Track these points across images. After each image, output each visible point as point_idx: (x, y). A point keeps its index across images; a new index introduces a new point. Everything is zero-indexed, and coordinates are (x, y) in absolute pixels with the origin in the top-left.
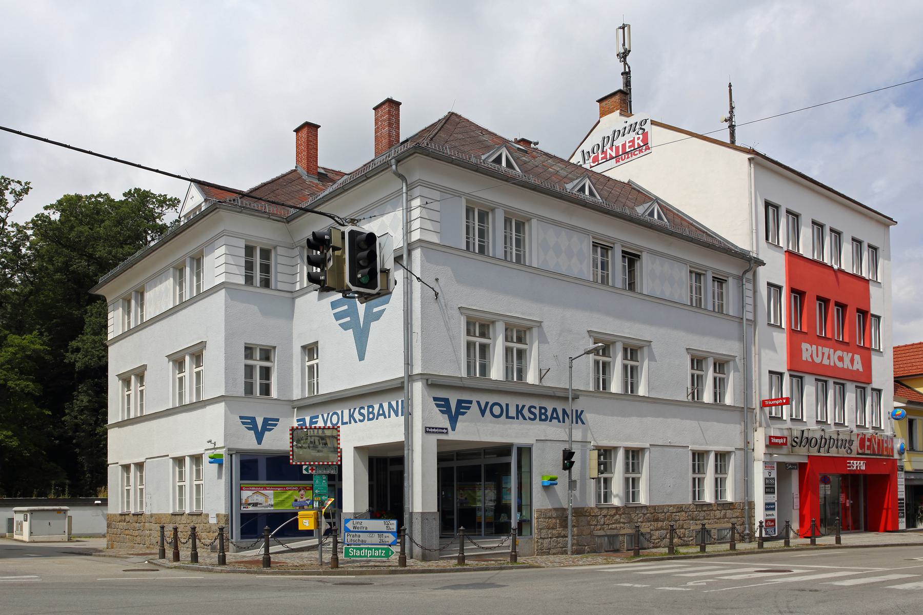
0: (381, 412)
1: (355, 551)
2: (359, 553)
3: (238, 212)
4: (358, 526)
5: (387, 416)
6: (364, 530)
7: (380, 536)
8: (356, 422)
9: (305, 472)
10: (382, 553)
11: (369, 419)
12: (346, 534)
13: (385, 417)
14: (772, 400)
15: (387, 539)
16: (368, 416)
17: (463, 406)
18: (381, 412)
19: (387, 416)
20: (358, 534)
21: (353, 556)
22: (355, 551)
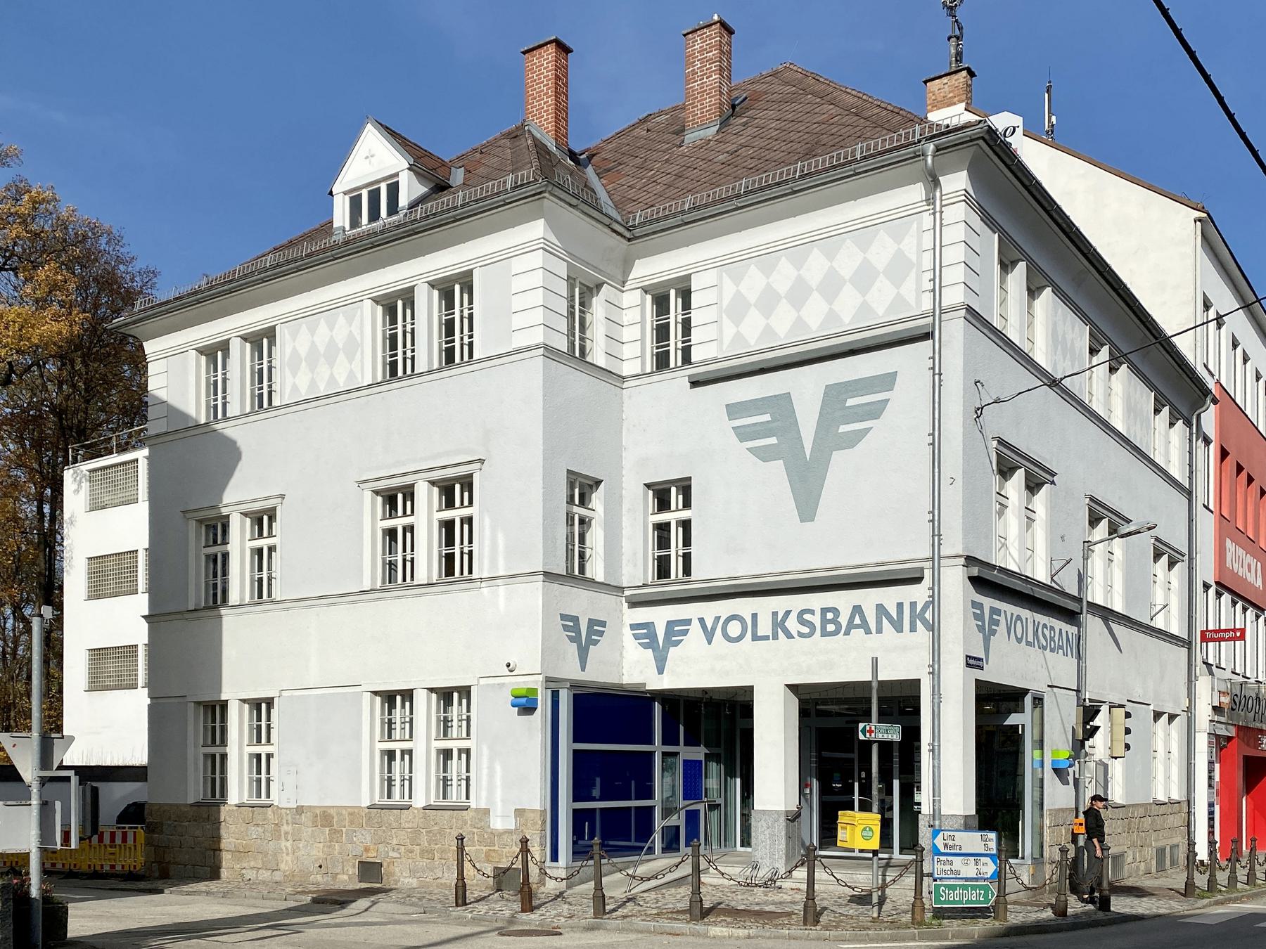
0: (857, 621)
1: (947, 892)
2: (952, 895)
3: (571, 205)
4: (951, 843)
5: (873, 629)
6: (958, 851)
7: (977, 863)
8: (789, 636)
9: (861, 737)
10: (980, 894)
11: (825, 633)
12: (936, 858)
13: (868, 632)
14: (1220, 631)
15: (984, 869)
16: (823, 628)
17: (676, 630)
18: (857, 621)
19: (873, 629)
20: (950, 858)
21: (945, 902)
22: (947, 892)
